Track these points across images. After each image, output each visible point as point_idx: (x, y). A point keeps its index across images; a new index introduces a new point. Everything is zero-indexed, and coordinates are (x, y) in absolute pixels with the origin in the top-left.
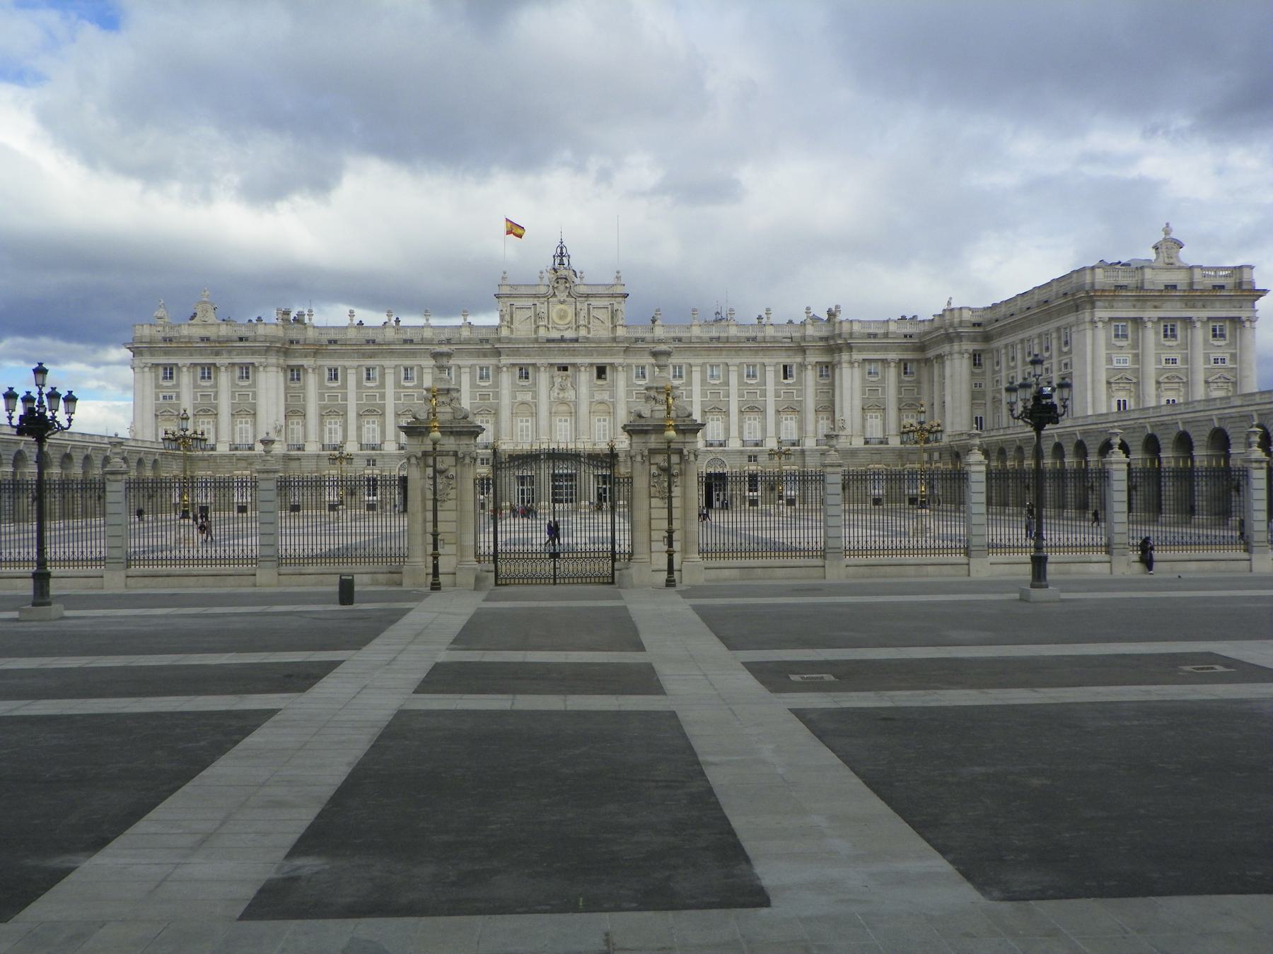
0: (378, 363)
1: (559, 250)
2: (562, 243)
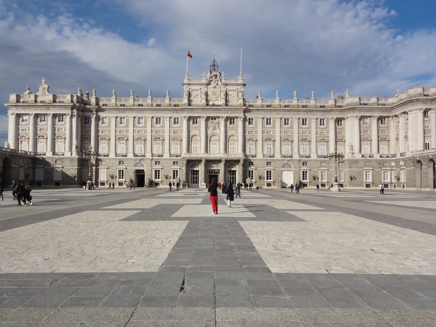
0: (126, 115)
2: (214, 60)
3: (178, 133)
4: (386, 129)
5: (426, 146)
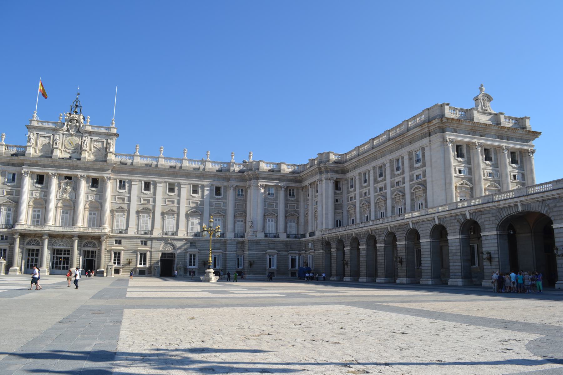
1: (75, 102)
3: (13, 195)
4: (295, 203)
5: (338, 224)
